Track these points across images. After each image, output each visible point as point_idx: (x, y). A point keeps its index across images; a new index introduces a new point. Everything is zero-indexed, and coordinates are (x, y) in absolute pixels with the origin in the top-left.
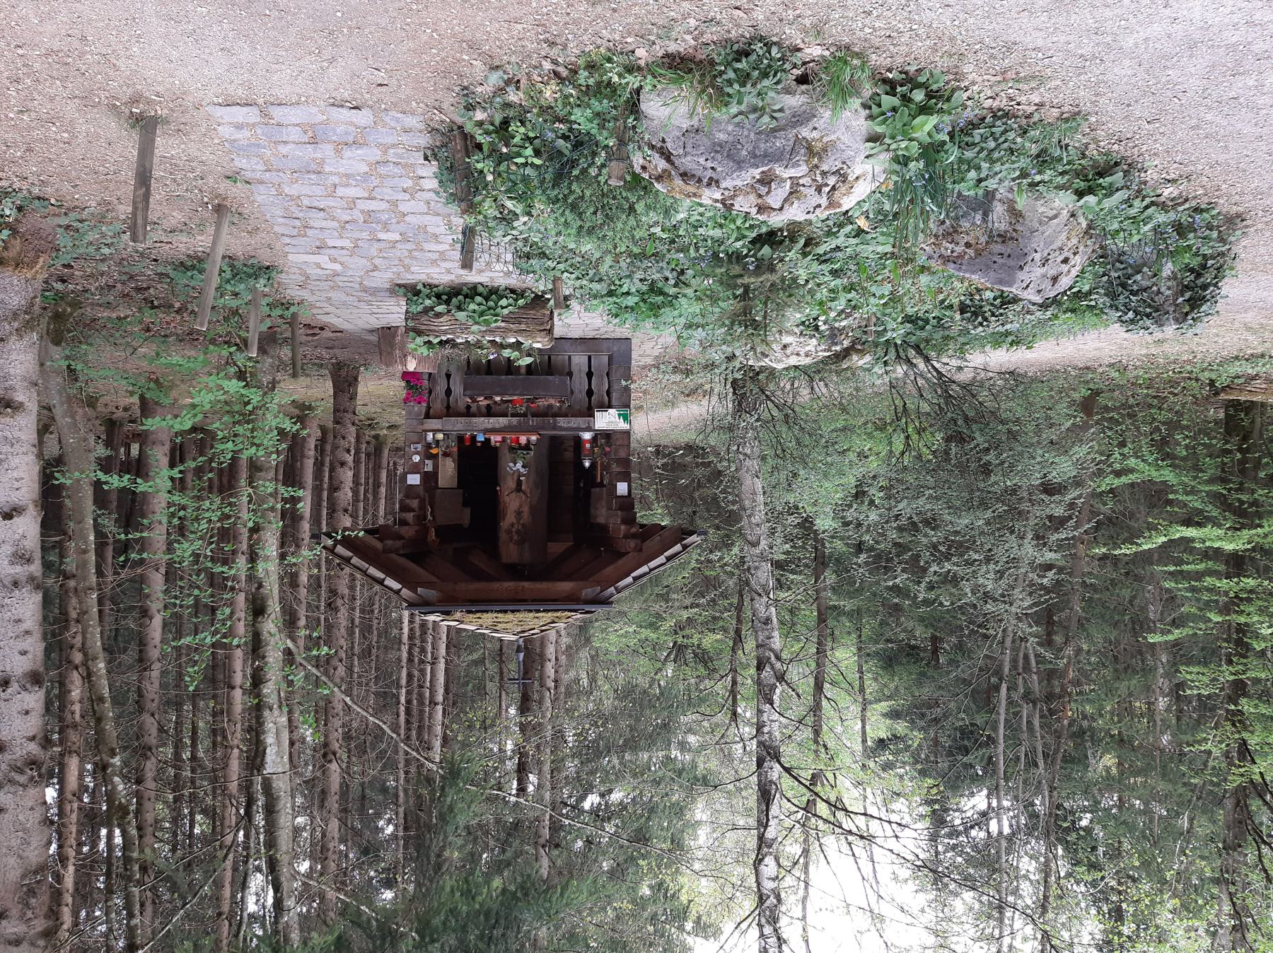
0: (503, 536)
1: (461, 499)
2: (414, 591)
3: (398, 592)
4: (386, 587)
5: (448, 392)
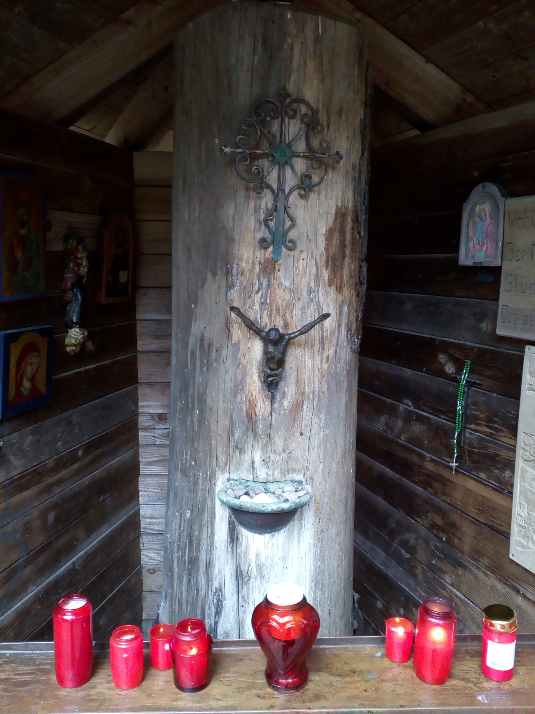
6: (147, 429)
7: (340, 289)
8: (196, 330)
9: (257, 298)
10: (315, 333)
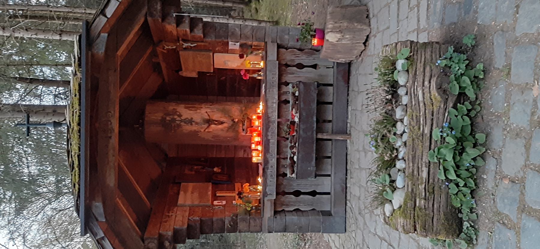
0: (171, 107)
2: (103, 30)
3: (103, 12)
5: (300, 66)
7: (202, 108)
8: (210, 139)
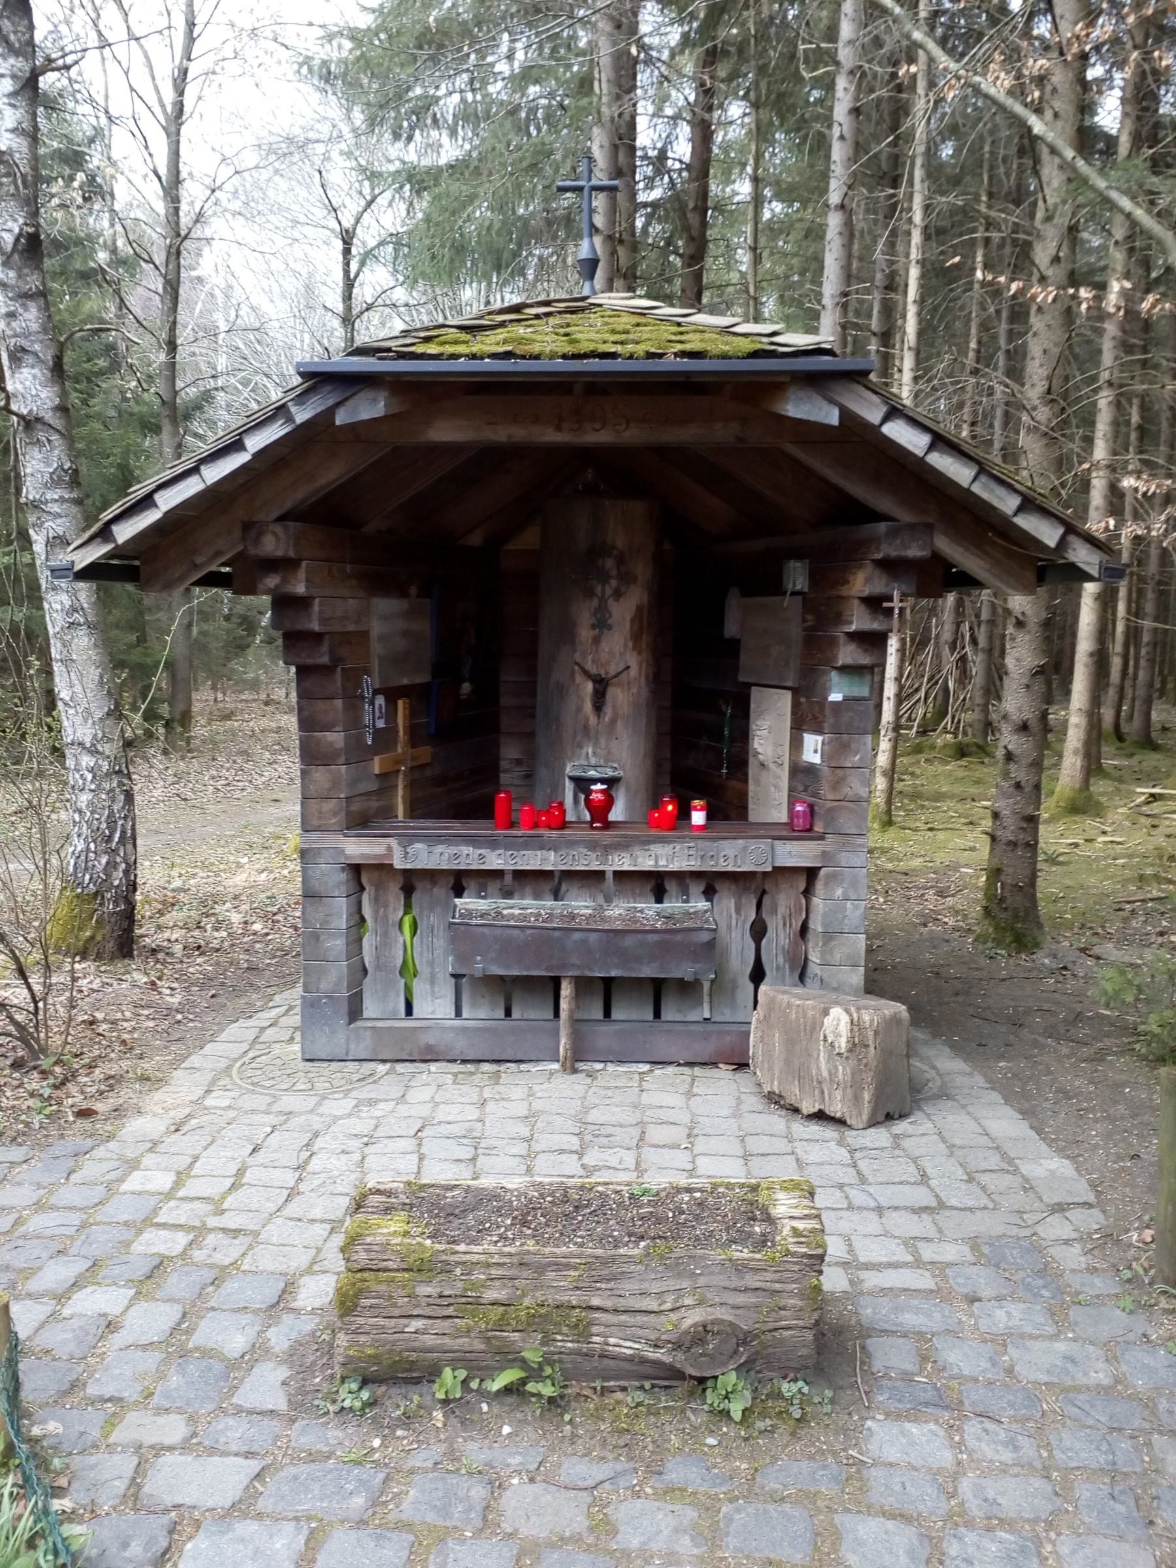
0: (642, 569)
1: (744, 659)
2: (845, 413)
4: (925, 428)
5: (758, 931)
6: (506, 771)
7: (640, 653)
9: (590, 658)
10: (624, 676)
